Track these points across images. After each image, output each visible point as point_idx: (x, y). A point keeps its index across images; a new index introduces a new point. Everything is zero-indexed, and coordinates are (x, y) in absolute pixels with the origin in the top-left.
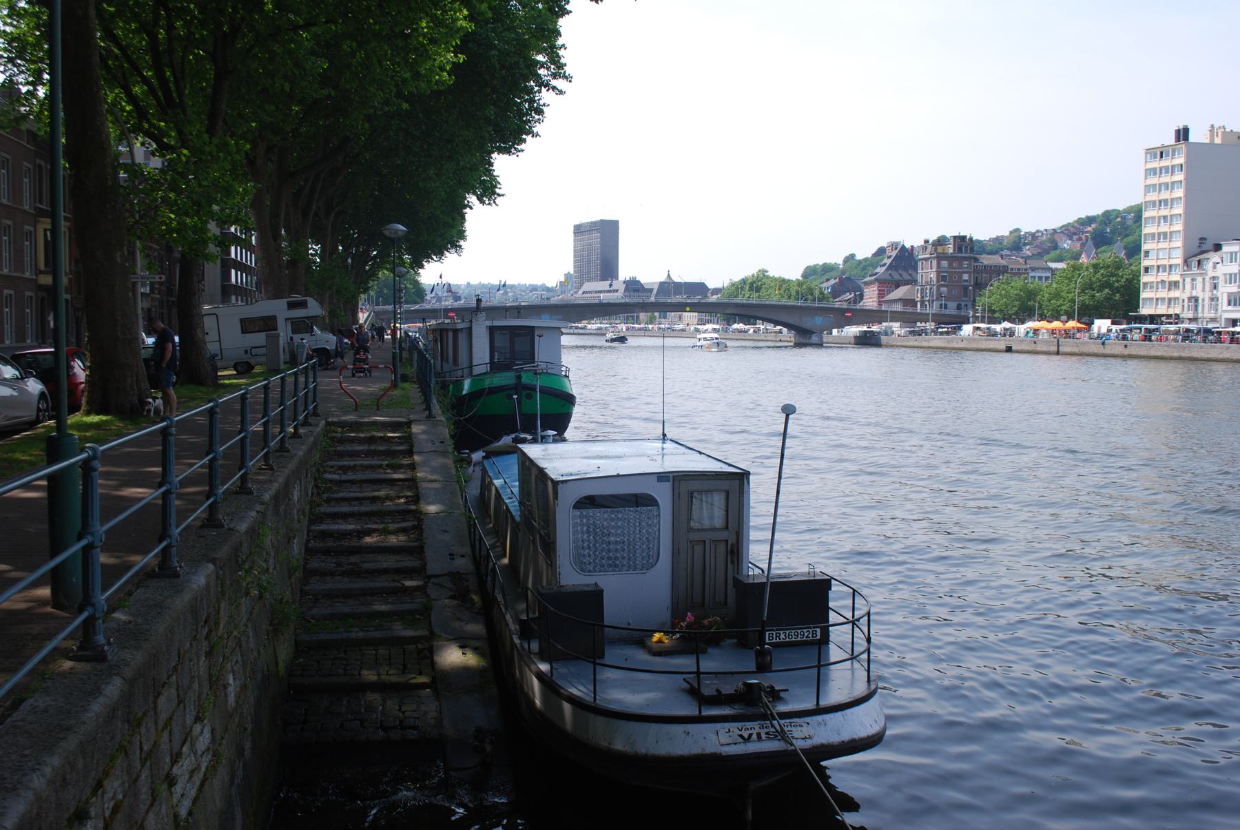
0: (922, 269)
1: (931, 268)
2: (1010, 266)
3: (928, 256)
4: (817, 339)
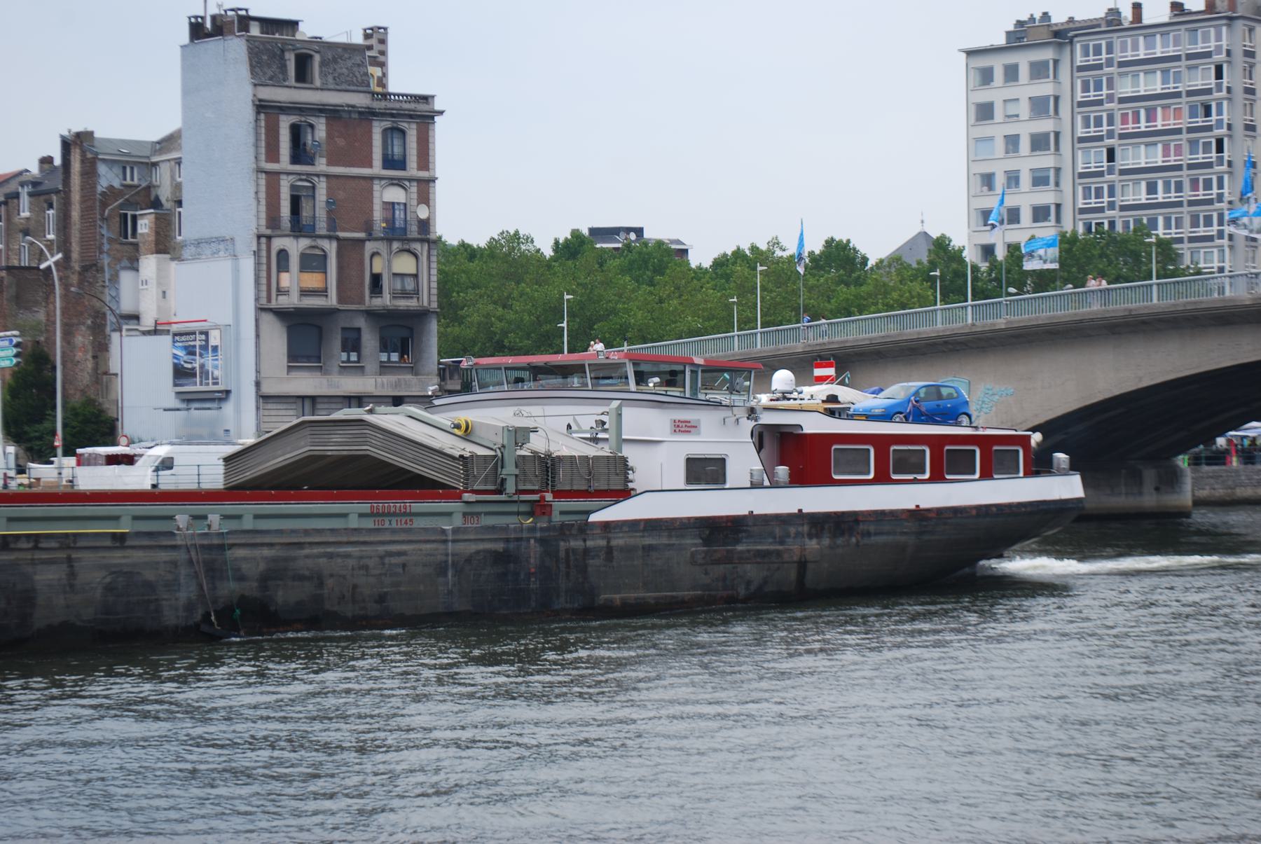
0: (300, 154)
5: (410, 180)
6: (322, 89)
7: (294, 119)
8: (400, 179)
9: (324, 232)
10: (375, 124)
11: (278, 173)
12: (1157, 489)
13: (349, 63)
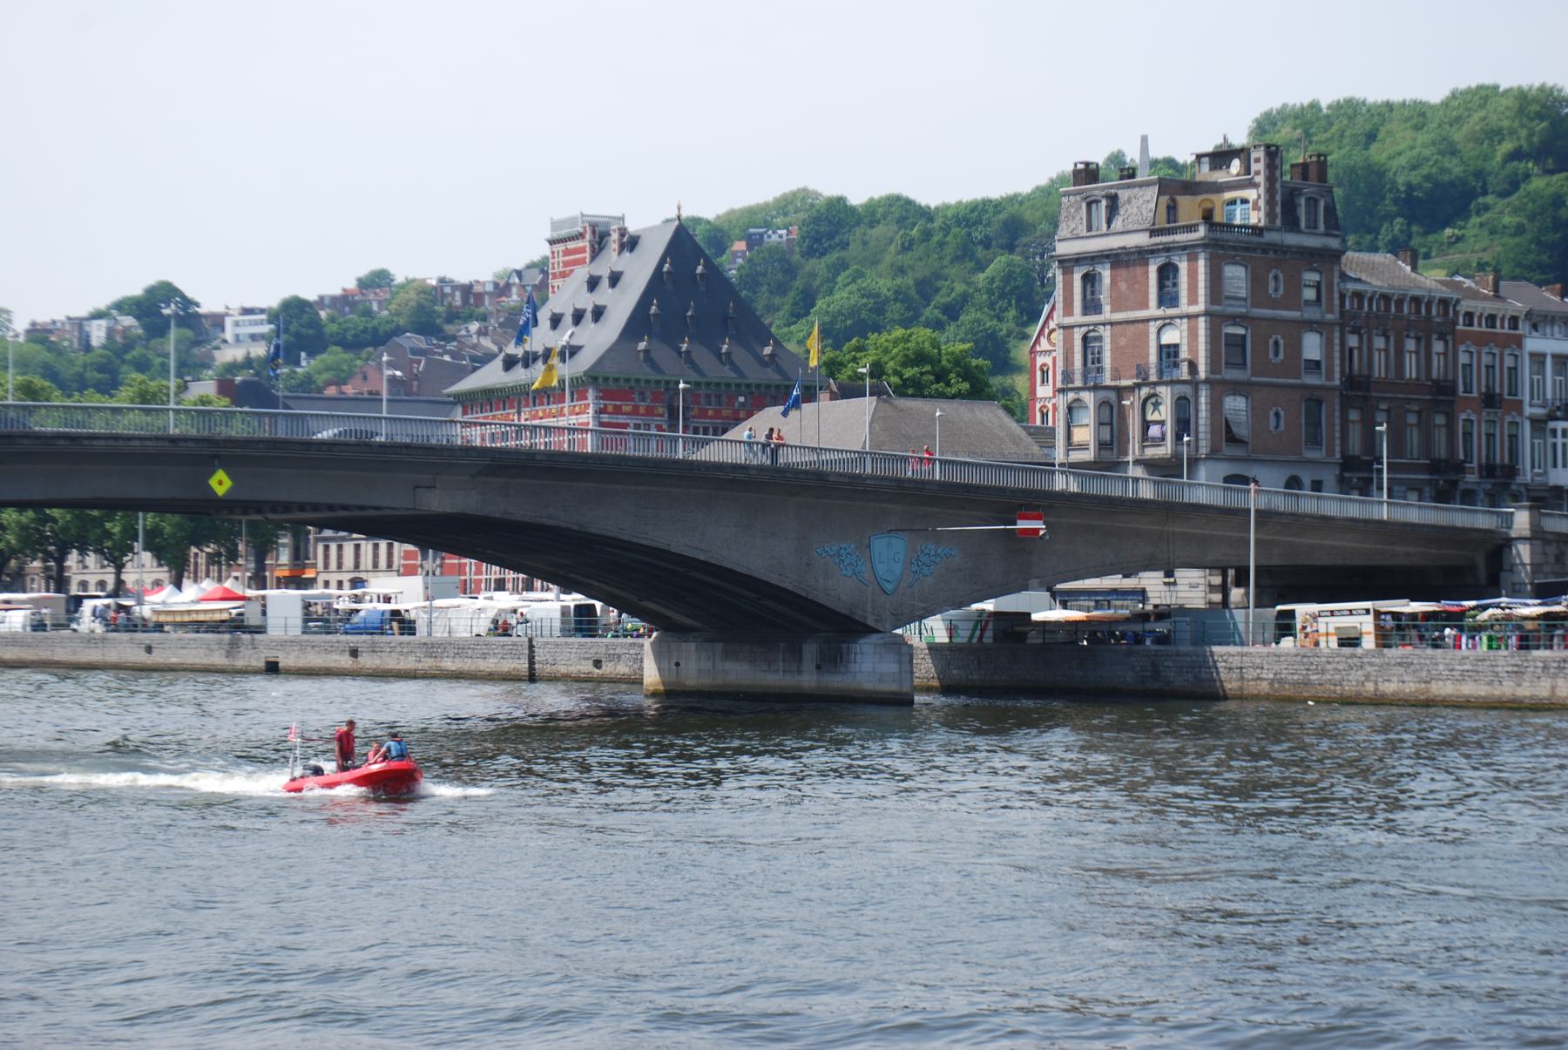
0: (1091, 306)
1: (1167, 297)
2: (1465, 306)
3: (1142, 240)
4: (889, 666)
5: (1181, 317)
9: (1108, 382)
10: (1151, 261)
11: (1072, 327)
12: (818, 667)
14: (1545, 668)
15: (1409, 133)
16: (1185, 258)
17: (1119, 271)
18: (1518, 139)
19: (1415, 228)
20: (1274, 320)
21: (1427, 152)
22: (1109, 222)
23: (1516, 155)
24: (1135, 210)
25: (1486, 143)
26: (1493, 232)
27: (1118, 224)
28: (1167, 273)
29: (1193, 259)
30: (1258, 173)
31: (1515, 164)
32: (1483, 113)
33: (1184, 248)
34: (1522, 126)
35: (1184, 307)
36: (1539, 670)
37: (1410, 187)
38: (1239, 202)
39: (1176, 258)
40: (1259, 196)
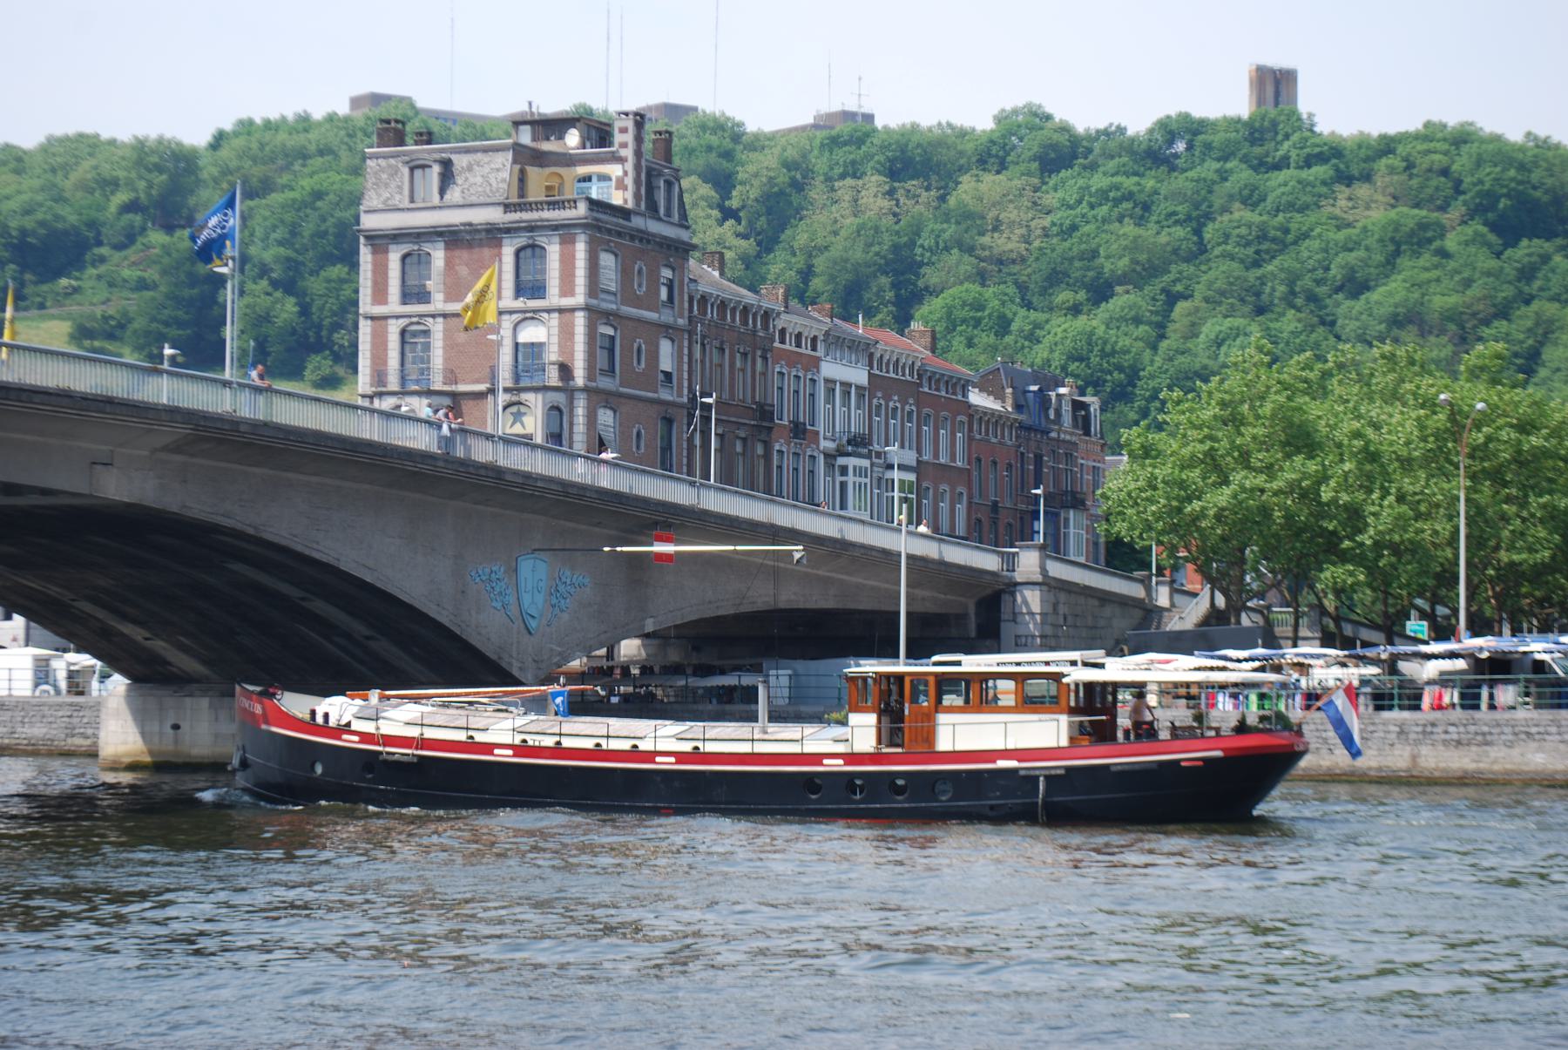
0: (414, 293)
1: (528, 287)
3: (495, 215)
5: (549, 311)
6: (440, 207)
7: (406, 248)
8: (535, 311)
9: (438, 385)
10: (505, 242)
11: (386, 318)
13: (486, 170)
14: (1401, 732)
15: (11, 177)
16: (557, 239)
17: (457, 253)
18: (135, 190)
19: (28, 276)
20: (639, 320)
21: (39, 198)
22: (442, 192)
23: (131, 207)
24: (479, 180)
25: (97, 194)
26: (111, 285)
27: (454, 195)
28: (530, 253)
29: (567, 241)
30: (624, 145)
31: (130, 216)
32: (93, 162)
33: (556, 228)
34: (141, 178)
35: (554, 298)
36: (1393, 736)
37: (24, 232)
38: (594, 179)
39: (544, 239)
40: (626, 173)
